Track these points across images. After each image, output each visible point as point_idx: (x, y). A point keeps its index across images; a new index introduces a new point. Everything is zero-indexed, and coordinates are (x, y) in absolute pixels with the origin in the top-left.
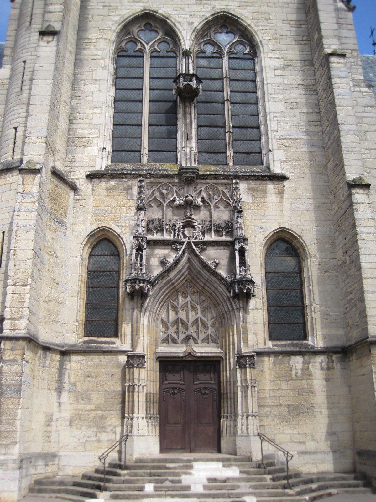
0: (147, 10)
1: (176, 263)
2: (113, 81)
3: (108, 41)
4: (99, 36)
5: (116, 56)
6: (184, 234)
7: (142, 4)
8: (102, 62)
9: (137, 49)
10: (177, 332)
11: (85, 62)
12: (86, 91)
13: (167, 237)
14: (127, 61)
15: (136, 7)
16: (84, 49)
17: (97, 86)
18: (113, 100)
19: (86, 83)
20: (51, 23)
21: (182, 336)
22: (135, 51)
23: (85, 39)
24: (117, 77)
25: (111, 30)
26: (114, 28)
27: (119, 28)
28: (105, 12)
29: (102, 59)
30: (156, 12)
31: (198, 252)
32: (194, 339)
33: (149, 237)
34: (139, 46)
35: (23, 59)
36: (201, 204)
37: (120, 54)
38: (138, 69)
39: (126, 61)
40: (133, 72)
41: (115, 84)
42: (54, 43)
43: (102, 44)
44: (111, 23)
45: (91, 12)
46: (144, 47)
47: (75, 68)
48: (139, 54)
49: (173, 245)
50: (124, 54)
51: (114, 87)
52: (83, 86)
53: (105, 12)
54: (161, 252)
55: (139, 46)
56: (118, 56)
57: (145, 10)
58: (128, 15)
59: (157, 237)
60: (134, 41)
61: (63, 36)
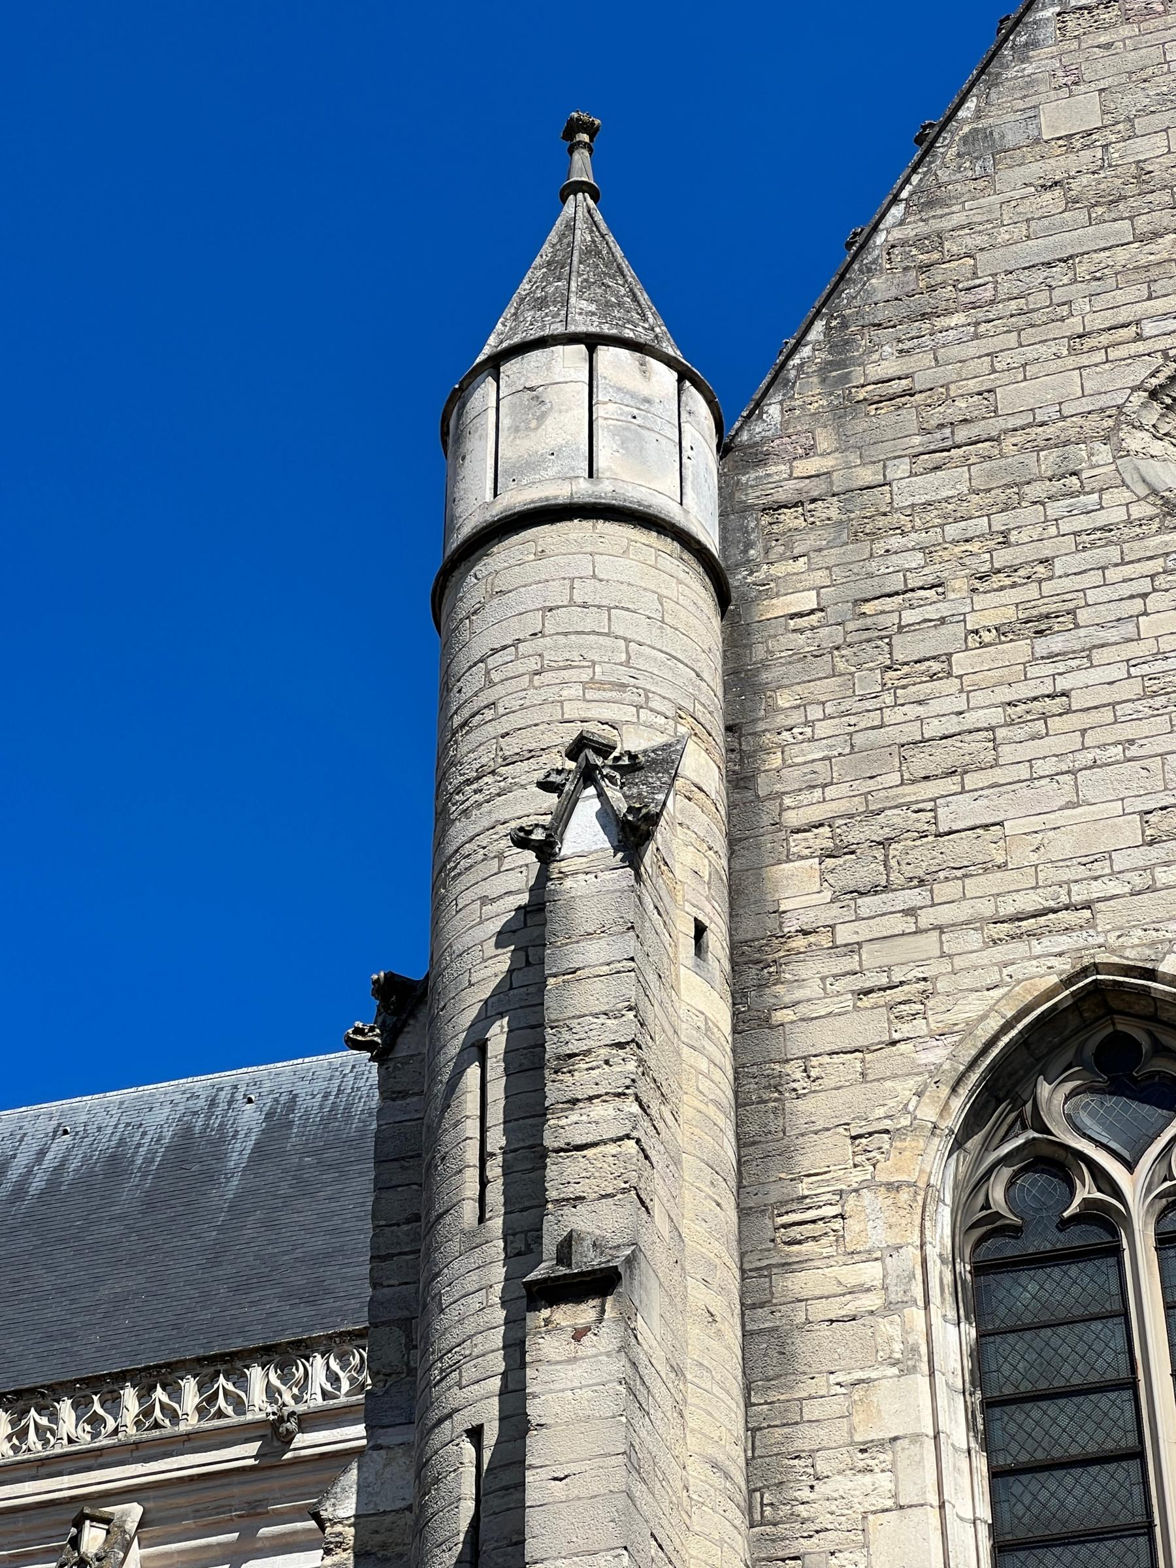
0: (1096, 968)
2: (971, 1426)
3: (904, 1196)
4: (856, 1177)
5: (964, 1268)
7: (1064, 942)
8: (889, 1328)
9: (1073, 1209)
11: (802, 1345)
12: (825, 1521)
14: (1033, 1287)
15: (1032, 967)
16: (787, 1267)
17: (884, 1481)
18: (986, 1544)
19: (822, 1467)
20: (579, 1220)
22: (1064, 1224)
23: (786, 1204)
24: (996, 1403)
25: (913, 1128)
26: (928, 1113)
27: (957, 1103)
28: (869, 1025)
29: (890, 1308)
30: (1151, 974)
34: (1087, 1190)
35: (464, 1420)
37: (994, 1258)
38: (1097, 1326)
39: (1027, 1292)
40: (1078, 1355)
41: (988, 1445)
42: (606, 1339)
43: (872, 1221)
44: (912, 1083)
45: (802, 1040)
46: (1117, 1193)
47: (748, 1389)
48: (1095, 1236)
50: (1010, 1248)
51: (981, 1463)
52: (805, 1494)
53: (869, 1025)
55: (1087, 1190)
56: (978, 1270)
57: (1084, 972)
58: (995, 1023)
60: (1057, 1164)
61: (650, 1292)
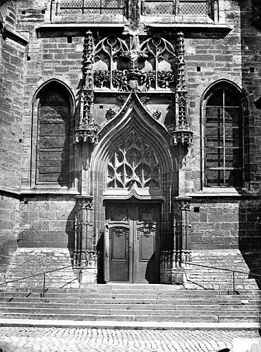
1: (121, 115)
6: (128, 86)
10: (122, 177)
13: (115, 90)
21: (127, 180)
31: (142, 103)
32: (137, 183)
33: (96, 90)
36: (146, 56)
49: (118, 99)
54: (107, 107)
59: (105, 90)
